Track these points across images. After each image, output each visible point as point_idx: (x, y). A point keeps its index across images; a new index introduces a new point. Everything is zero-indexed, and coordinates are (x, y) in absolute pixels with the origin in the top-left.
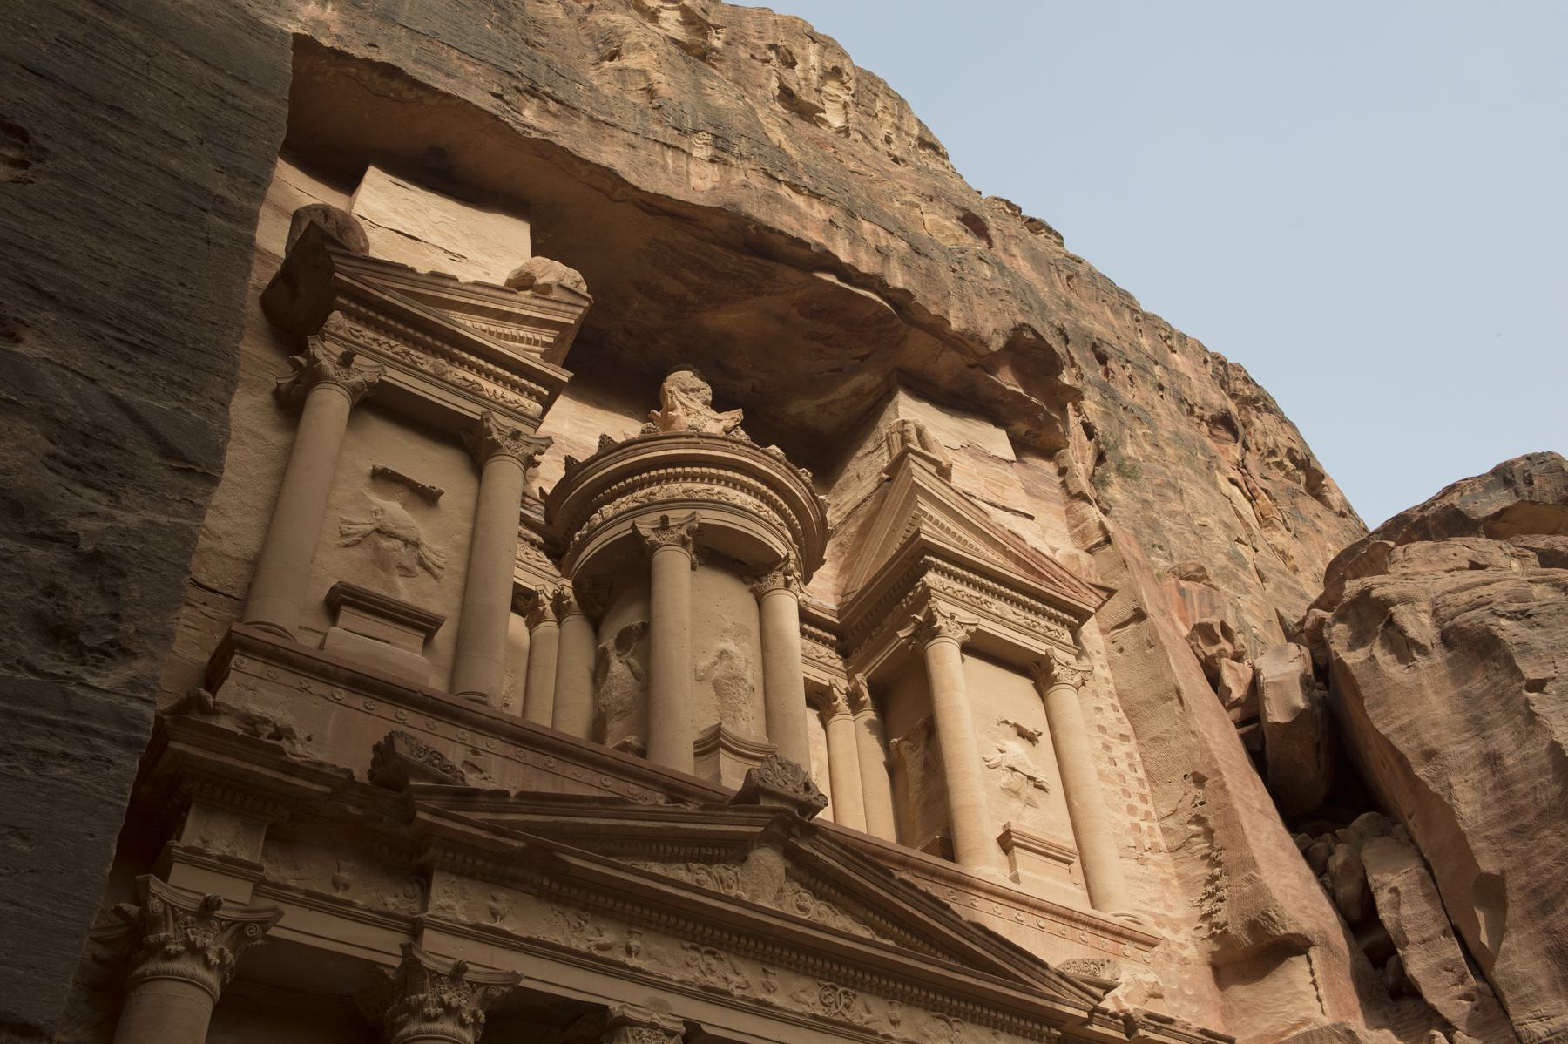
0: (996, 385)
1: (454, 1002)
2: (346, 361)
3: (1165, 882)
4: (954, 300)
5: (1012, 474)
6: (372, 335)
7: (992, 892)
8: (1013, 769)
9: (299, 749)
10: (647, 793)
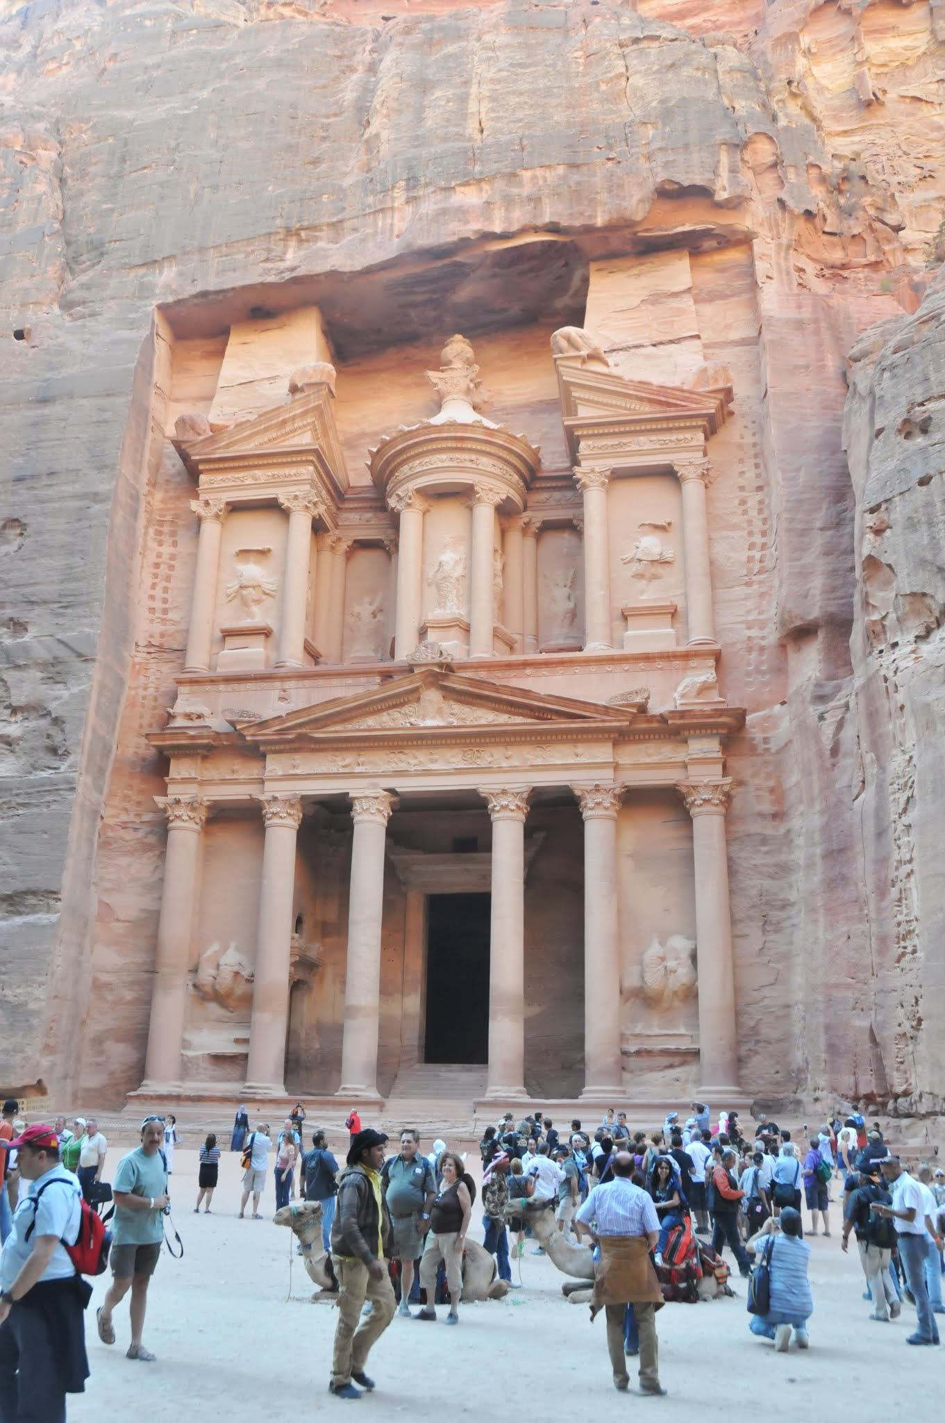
1: (274, 810)
2: (207, 503)
3: (762, 595)
5: (688, 302)
6: (220, 477)
7: (588, 662)
8: (640, 560)
9: (207, 722)
10: (371, 679)
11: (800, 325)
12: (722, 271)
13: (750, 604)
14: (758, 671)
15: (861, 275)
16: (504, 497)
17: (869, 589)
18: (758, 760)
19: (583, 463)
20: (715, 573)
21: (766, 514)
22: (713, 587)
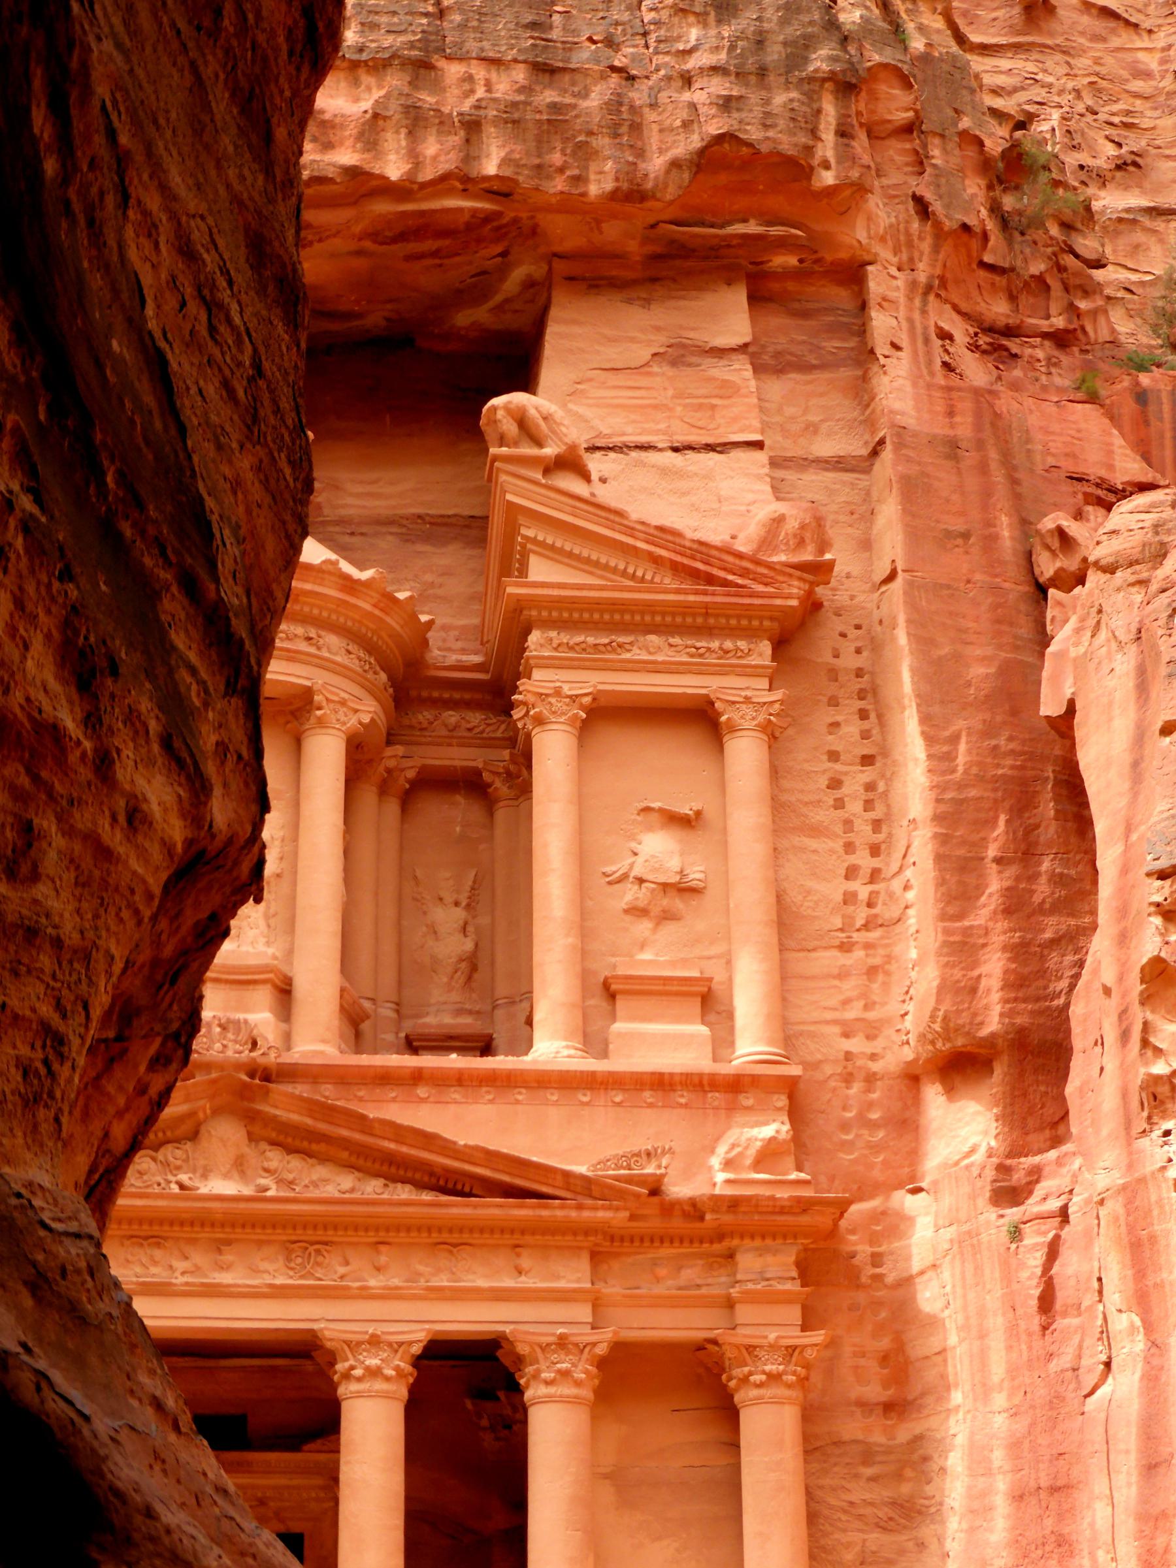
0: (696, 236)
3: (872, 971)
4: (602, 142)
5: (740, 371)
8: (641, 881)
11: (952, 448)
12: (805, 314)
13: (849, 987)
14: (863, 1121)
15: (1040, 354)
16: (366, 719)
17: (1150, 1016)
18: (861, 1297)
19: (537, 674)
20: (786, 923)
21: (878, 812)
22: (782, 948)
